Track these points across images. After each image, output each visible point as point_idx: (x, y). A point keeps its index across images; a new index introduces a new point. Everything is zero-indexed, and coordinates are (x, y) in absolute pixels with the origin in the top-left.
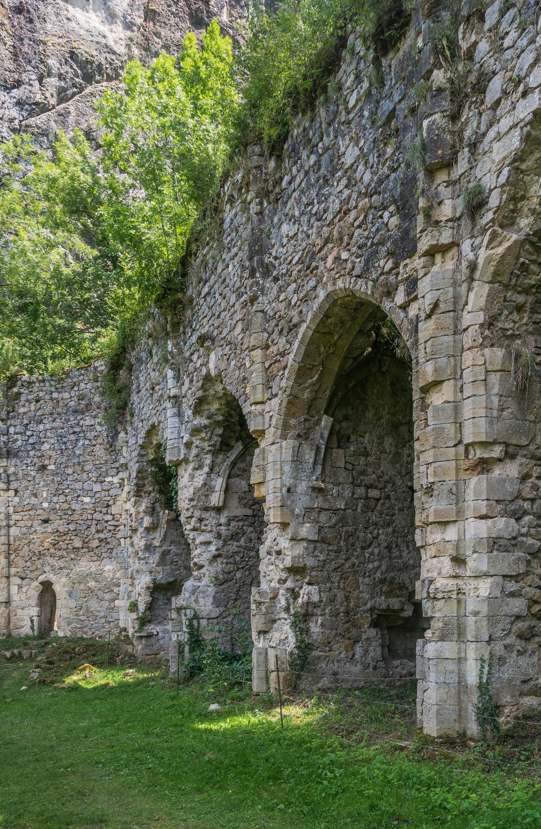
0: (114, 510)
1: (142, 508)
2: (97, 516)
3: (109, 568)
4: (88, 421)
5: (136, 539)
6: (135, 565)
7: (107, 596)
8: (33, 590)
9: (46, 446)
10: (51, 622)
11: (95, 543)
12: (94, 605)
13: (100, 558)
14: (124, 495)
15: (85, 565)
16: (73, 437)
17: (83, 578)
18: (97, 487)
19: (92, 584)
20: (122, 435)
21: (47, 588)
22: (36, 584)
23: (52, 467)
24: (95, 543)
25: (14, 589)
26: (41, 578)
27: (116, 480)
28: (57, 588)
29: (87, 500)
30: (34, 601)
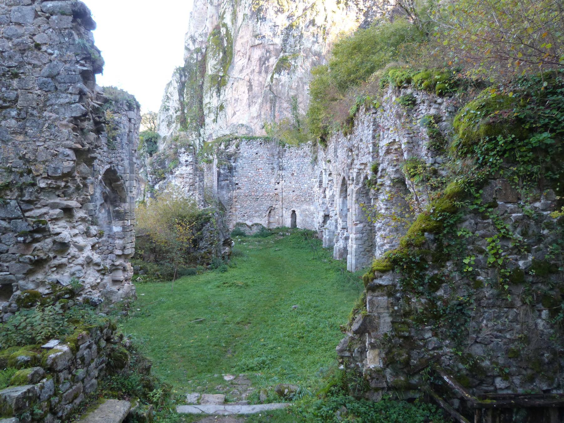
0: (314, 189)
1: (321, 191)
2: (309, 191)
3: (312, 208)
4: (306, 160)
5: (320, 200)
6: (319, 209)
7: (312, 217)
8: (290, 213)
9: (293, 168)
10: (295, 222)
11: (308, 200)
12: (307, 219)
13: (309, 205)
14: (316, 186)
15: (305, 207)
16: (302, 165)
17: (304, 211)
18: (309, 182)
19: (307, 213)
20: (316, 166)
21: (294, 211)
22: (290, 211)
23: (295, 174)
24: (308, 200)
25: (284, 212)
26: (292, 209)
27: (314, 180)
28: (296, 213)
29: (306, 185)
30: (290, 216)
